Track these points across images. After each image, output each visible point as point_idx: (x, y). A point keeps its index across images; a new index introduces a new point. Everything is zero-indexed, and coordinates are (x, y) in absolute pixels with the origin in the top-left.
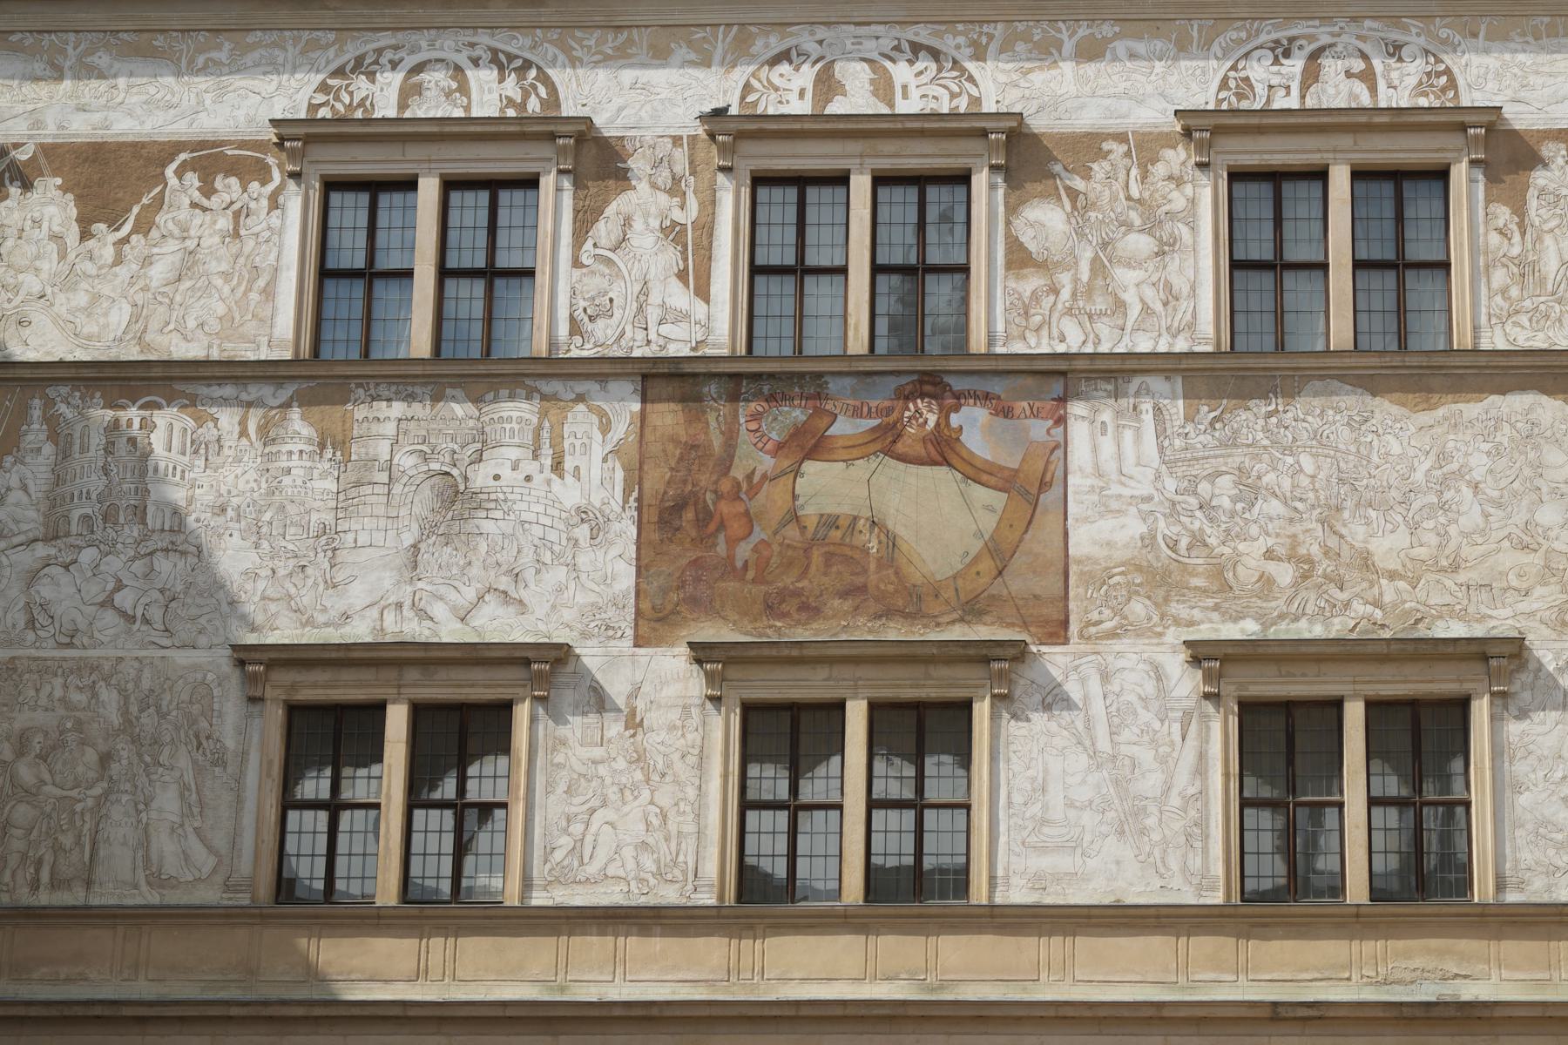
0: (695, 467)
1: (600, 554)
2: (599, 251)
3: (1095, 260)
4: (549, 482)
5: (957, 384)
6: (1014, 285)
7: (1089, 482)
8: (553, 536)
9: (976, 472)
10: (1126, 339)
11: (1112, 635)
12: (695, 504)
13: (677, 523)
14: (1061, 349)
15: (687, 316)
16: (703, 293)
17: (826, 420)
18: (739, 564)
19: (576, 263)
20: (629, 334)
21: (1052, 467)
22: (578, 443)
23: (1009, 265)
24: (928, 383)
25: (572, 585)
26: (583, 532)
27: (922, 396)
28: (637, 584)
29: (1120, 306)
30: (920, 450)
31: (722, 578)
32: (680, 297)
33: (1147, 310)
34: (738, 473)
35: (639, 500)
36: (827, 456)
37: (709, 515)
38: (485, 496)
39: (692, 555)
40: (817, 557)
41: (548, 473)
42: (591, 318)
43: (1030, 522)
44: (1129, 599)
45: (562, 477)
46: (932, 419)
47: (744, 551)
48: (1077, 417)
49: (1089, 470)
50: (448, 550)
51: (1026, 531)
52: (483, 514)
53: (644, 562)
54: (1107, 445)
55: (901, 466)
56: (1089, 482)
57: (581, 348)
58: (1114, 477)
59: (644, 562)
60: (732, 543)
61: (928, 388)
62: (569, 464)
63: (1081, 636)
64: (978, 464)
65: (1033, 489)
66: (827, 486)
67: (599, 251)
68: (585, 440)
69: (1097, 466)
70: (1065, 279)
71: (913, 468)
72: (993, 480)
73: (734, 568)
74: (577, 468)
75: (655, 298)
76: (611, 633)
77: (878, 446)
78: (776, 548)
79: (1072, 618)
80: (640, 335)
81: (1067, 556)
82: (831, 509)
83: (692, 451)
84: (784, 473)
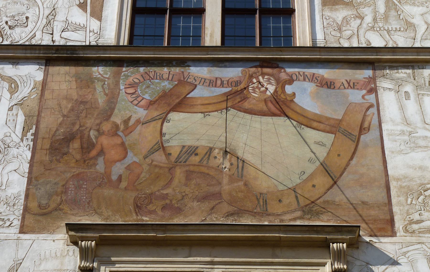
0: (83, 115)
6: (329, 14)
12: (81, 138)
15: (84, 28)
17: (188, 88)
18: (114, 178)
21: (368, 119)
27: (263, 75)
28: (27, 189)
29: (410, 26)
30: (262, 106)
32: (79, 17)
34: (117, 119)
35: (35, 135)
36: (188, 110)
37: (92, 145)
39: (76, 171)
40: (179, 173)
43: (354, 153)
46: (271, 89)
48: (384, 89)
51: (352, 158)
53: (34, 175)
54: (411, 106)
55: (248, 116)
56: (399, 128)
58: (420, 124)
59: (34, 175)
60: (109, 164)
61: (266, 70)
63: (406, 230)
65: (356, 131)
72: (322, 126)
73: (110, 181)
75: (61, 17)
79: (397, 218)
82: (190, 142)
83: (82, 106)
84: (154, 120)
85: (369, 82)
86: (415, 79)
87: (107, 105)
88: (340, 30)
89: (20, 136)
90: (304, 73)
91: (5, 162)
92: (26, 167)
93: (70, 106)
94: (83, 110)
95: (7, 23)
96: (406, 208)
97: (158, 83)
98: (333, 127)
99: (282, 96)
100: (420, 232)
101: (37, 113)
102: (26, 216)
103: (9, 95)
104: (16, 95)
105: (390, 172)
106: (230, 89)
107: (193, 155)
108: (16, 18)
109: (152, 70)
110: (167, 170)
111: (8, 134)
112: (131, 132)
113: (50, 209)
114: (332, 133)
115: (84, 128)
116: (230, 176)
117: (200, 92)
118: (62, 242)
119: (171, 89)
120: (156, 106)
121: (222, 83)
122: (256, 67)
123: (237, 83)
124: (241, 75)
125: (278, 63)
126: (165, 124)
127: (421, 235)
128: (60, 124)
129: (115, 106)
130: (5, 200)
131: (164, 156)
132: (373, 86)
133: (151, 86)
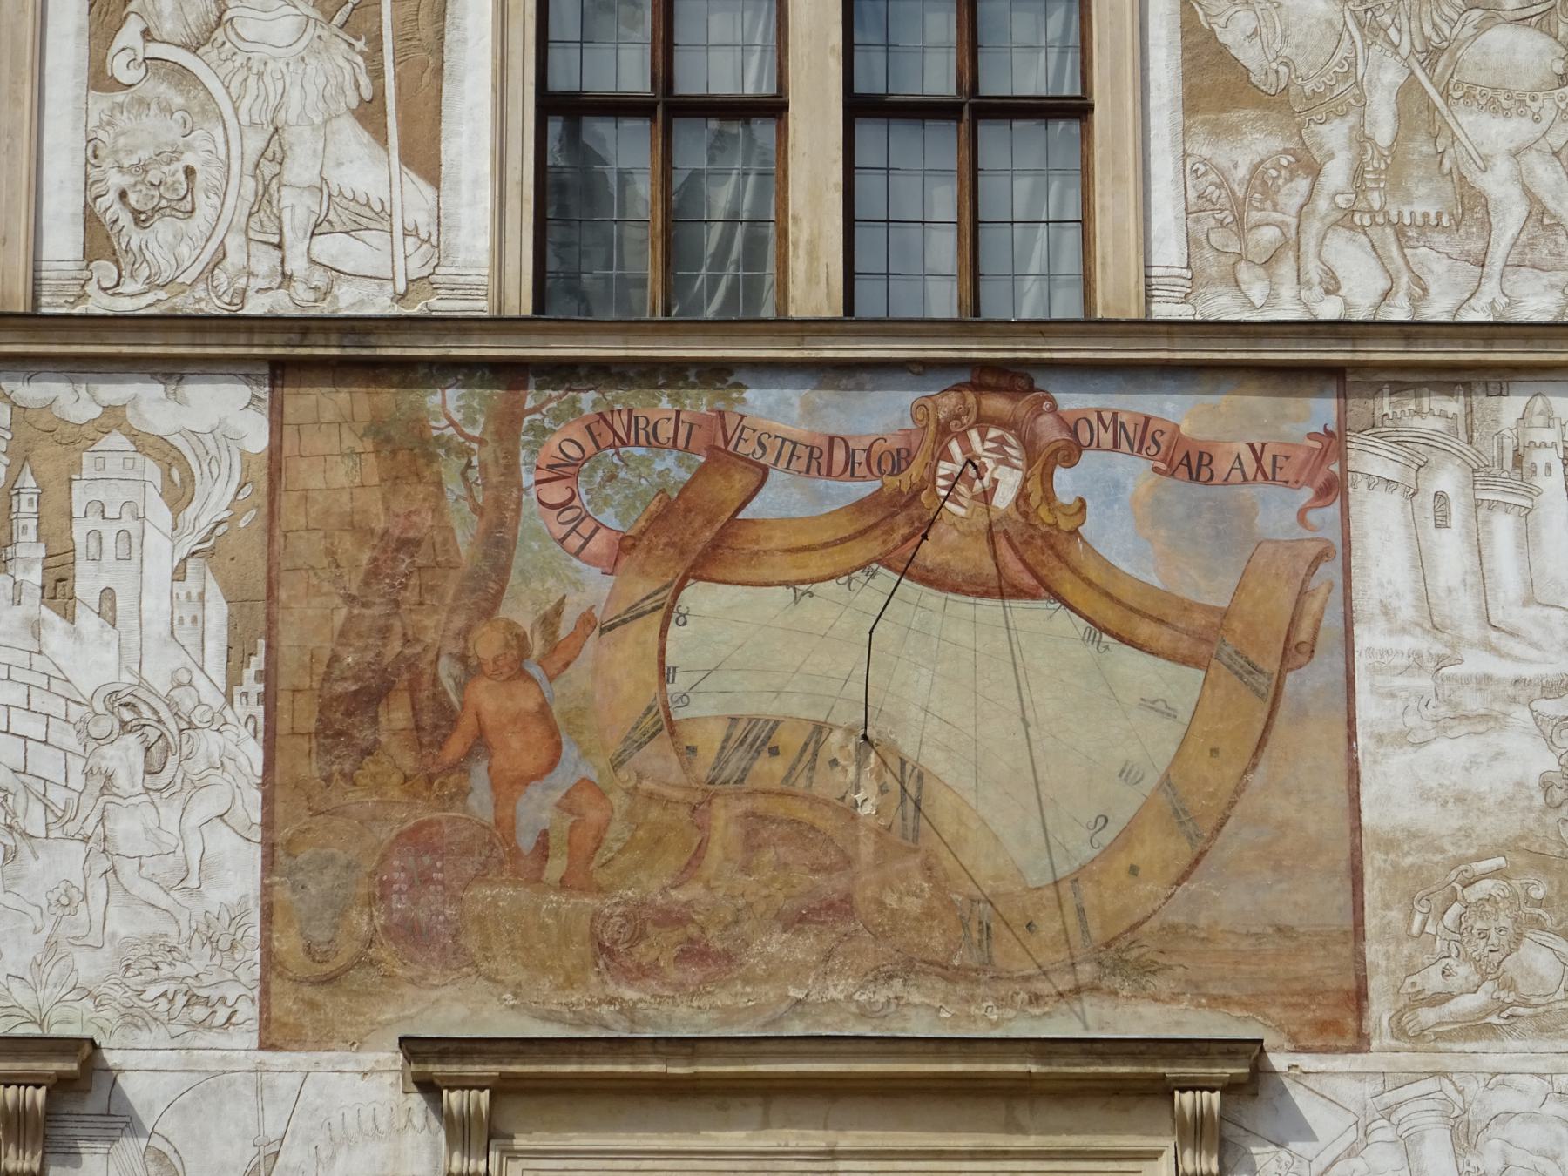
0: (411, 596)
1: (170, 816)
2: (155, 50)
3: (1408, 91)
4: (35, 628)
5: (1073, 400)
6: (1206, 151)
7: (1408, 643)
8: (46, 763)
9: (1123, 618)
10: (1490, 289)
11: (1477, 1028)
12: (413, 688)
13: (364, 735)
14: (1329, 310)
15: (383, 215)
16: (423, 157)
17: (742, 480)
18: (527, 842)
19: (100, 79)
20: (235, 258)
21: (1313, 605)
22: (109, 531)
23: (1192, 102)
24: (996, 389)
25: (98, 891)
26: (124, 757)
27: (983, 422)
28: (266, 890)
29: (1472, 206)
30: (978, 558)
31: (481, 877)
32: (365, 170)
33: (1539, 215)
34: (520, 611)
35: (268, 676)
36: (744, 574)
37: (448, 717)
39: (404, 816)
40: (724, 821)
41: (32, 605)
42: (141, 219)
43: (1262, 743)
44: (1518, 939)
45: (68, 615)
46: (1008, 484)
47: (537, 809)
48: (1373, 481)
49: (1406, 611)
53: (282, 835)
54: (1450, 549)
55: (933, 598)
56: (1408, 643)
57: (112, 291)
58: (1471, 630)
60: (508, 786)
62: (86, 584)
63: (1399, 1032)
64: (1128, 598)
65: (1271, 656)
66: (748, 647)
67: (155, 50)
68: (128, 523)
69: (1425, 599)
70: (1334, 135)
71: (962, 605)
72: (1164, 637)
73: (515, 854)
74: (108, 594)
75: (301, 170)
76: (199, 1012)
77: (873, 547)
78: (618, 800)
79: (1375, 985)
80: (264, 261)
81: (1357, 828)
83: (400, 558)
84: (635, 614)
85: (1324, 455)
86: (1470, 443)
87: (485, 556)
88: (1240, 226)
89: (222, 686)
90: (1115, 414)
91: (188, 787)
92: (251, 805)
93: (365, 557)
94: (408, 576)
95: (123, 195)
96: (1407, 948)
97: (642, 460)
98: (1197, 639)
99: (1043, 512)
100: (1439, 1037)
101: (262, 587)
102: (274, 988)
103: (168, 516)
104: (190, 512)
105: (1366, 817)
106: (877, 484)
107: (765, 754)
108: (154, 176)
109: (622, 398)
110: (684, 812)
111: (185, 679)
112: (566, 665)
113: (341, 961)
114: (1198, 665)
115: (418, 649)
116: (879, 834)
117: (782, 500)
118: (389, 1078)
119: (687, 486)
120: (639, 555)
121: (850, 455)
122: (957, 388)
123: (901, 459)
124: (909, 425)
125: (1032, 373)
126: (673, 630)
127: (1441, 1045)
128: (343, 633)
129: (510, 557)
130: (203, 928)
131: (673, 756)
132: (1335, 468)
133: (622, 474)
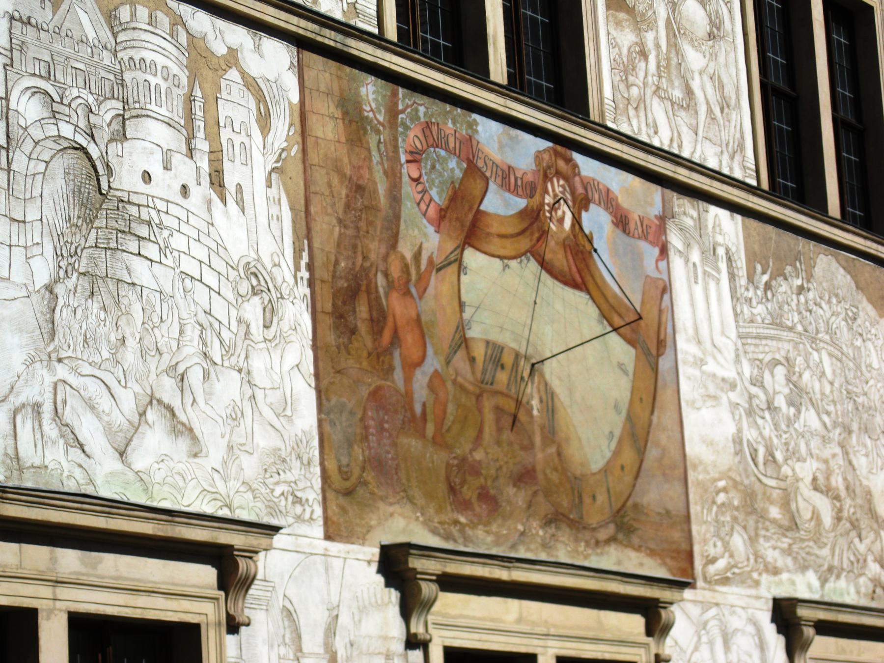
8: (220, 310)
12: (368, 293)
38: (133, 210)
50: (94, 307)
52: (133, 246)
